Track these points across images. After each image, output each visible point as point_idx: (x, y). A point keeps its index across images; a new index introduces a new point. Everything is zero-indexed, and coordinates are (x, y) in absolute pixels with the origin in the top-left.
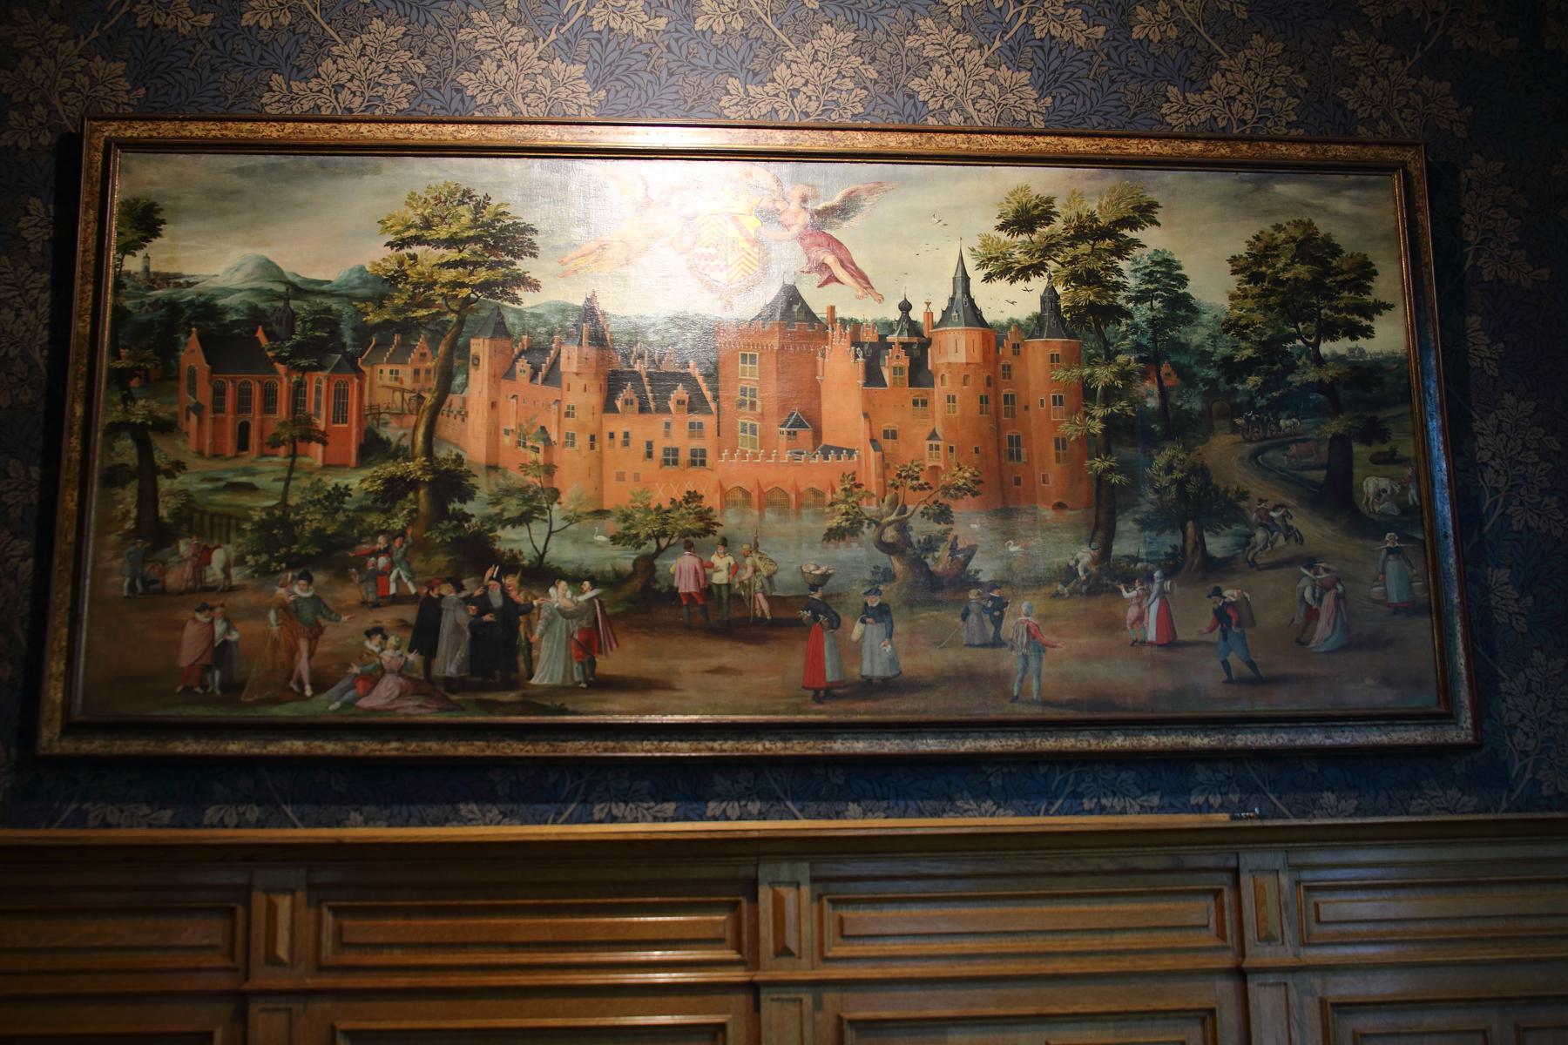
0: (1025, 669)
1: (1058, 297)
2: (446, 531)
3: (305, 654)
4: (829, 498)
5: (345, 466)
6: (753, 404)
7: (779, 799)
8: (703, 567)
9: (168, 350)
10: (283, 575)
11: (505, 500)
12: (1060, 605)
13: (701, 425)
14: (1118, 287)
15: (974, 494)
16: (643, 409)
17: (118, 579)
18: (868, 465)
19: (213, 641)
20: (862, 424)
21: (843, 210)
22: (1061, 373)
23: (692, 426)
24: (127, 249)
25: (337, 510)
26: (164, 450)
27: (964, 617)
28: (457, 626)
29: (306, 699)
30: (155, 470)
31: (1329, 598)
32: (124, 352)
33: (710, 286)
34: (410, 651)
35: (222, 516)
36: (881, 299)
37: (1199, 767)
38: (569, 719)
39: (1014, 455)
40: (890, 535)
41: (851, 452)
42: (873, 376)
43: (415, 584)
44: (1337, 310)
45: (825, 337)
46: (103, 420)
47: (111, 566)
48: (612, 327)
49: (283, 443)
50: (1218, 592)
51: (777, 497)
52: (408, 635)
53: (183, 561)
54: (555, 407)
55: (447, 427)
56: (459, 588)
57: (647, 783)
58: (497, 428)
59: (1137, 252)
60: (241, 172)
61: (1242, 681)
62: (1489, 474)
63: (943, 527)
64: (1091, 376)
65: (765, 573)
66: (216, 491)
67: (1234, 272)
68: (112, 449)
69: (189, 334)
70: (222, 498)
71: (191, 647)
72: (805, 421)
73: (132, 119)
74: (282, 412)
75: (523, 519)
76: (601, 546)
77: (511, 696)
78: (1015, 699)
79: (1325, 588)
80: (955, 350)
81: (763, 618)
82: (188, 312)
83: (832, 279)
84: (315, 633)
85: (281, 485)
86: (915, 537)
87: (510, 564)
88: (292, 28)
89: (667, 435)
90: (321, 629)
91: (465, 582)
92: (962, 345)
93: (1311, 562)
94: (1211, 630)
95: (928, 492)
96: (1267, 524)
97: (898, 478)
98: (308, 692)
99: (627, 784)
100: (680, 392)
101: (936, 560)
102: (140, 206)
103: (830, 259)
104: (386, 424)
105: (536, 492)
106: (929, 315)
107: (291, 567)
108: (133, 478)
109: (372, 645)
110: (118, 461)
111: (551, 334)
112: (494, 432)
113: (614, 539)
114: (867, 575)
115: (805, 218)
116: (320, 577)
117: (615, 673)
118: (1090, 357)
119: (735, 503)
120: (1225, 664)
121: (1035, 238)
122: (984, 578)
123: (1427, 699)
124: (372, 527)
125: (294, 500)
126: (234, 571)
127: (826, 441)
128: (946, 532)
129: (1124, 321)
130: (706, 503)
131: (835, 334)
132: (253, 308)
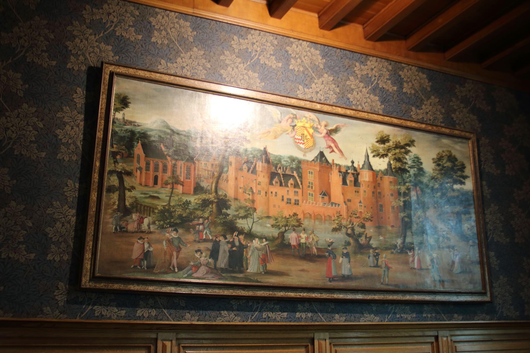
0: (384, 274)
1: (391, 164)
2: (222, 219)
3: (175, 257)
4: (333, 218)
5: (190, 194)
6: (312, 187)
7: (316, 312)
8: (298, 237)
9: (130, 146)
10: (168, 229)
11: (240, 210)
12: (393, 256)
13: (297, 192)
14: (406, 163)
15: (371, 221)
16: (281, 185)
17: (111, 226)
18: (343, 208)
19: (144, 250)
20: (342, 196)
21: (336, 130)
22: (392, 187)
23: (295, 192)
24: (117, 110)
25: (187, 209)
26: (128, 181)
27: (369, 257)
28: (225, 251)
29: (176, 273)
30: (125, 189)
32: (115, 146)
33: (300, 149)
34: (210, 258)
35: (147, 207)
36: (346, 159)
37: (425, 306)
38: (259, 284)
39: (381, 210)
40: (349, 231)
41: (339, 205)
42: (344, 182)
43: (212, 236)
44: (458, 176)
45: (331, 168)
46: (107, 169)
47: (109, 222)
48: (272, 159)
49: (169, 184)
51: (319, 217)
52: (209, 253)
53: (134, 221)
54: (255, 181)
55: (222, 184)
56: (226, 238)
57: (278, 306)
58: (237, 186)
59: (410, 154)
60: (155, 89)
62: (489, 225)
63: (363, 230)
64: (400, 188)
65: (315, 240)
66: (146, 198)
67: (434, 163)
68: (110, 179)
69: (138, 142)
70: (148, 201)
71: (136, 253)
72: (326, 194)
73: (119, 66)
74: (169, 173)
75: (245, 217)
76: (269, 228)
77: (241, 275)
78: (382, 284)
80: (365, 177)
81: (315, 255)
82: (138, 135)
83: (333, 151)
84: (179, 250)
85: (168, 198)
86: (356, 232)
87: (241, 232)
88: (168, 45)
89: (288, 194)
90: (180, 249)
91: (227, 236)
92: (367, 176)
95: (359, 219)
97: (352, 214)
98: (176, 270)
99: (273, 306)
100: (291, 181)
101: (362, 240)
102: (122, 96)
103: (332, 145)
104: (203, 181)
105: (249, 209)
106: (359, 165)
107: (171, 226)
108: (117, 190)
109: (197, 255)
110: (112, 184)
111: (254, 157)
112: (236, 187)
113: (273, 226)
114: (343, 243)
115: (325, 132)
116: (180, 231)
117: (272, 269)
118: (400, 183)
119: (307, 218)
121: (385, 146)
122: (374, 246)
123: (479, 288)
124: (198, 215)
125: (172, 204)
126: (151, 226)
127: (332, 201)
128: (364, 232)
129: (408, 173)
130: (299, 217)
131: (334, 168)
132: (160, 136)
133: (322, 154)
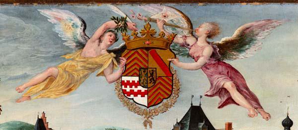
21: (241, 43)
33: (134, 108)
83: (230, 101)
103: (228, 85)
115: (208, 51)
133: (196, 114)
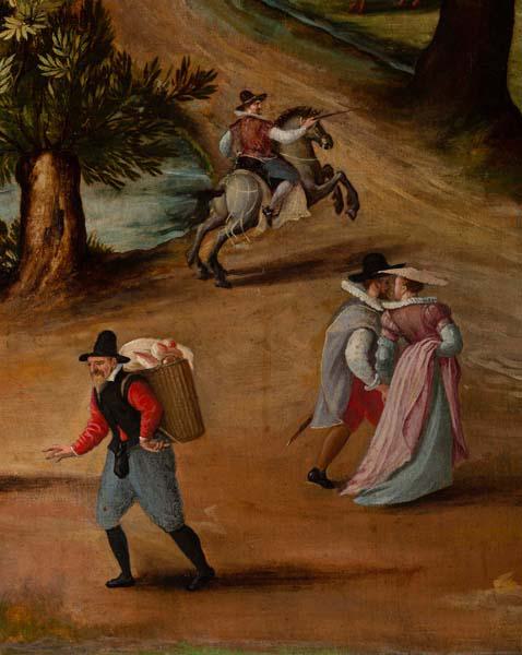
31: (414, 361)
50: (107, 345)
61: (164, 582)
79: (405, 337)
93: (371, 266)
94: (83, 448)
96: (262, 163)
120: (117, 539)
